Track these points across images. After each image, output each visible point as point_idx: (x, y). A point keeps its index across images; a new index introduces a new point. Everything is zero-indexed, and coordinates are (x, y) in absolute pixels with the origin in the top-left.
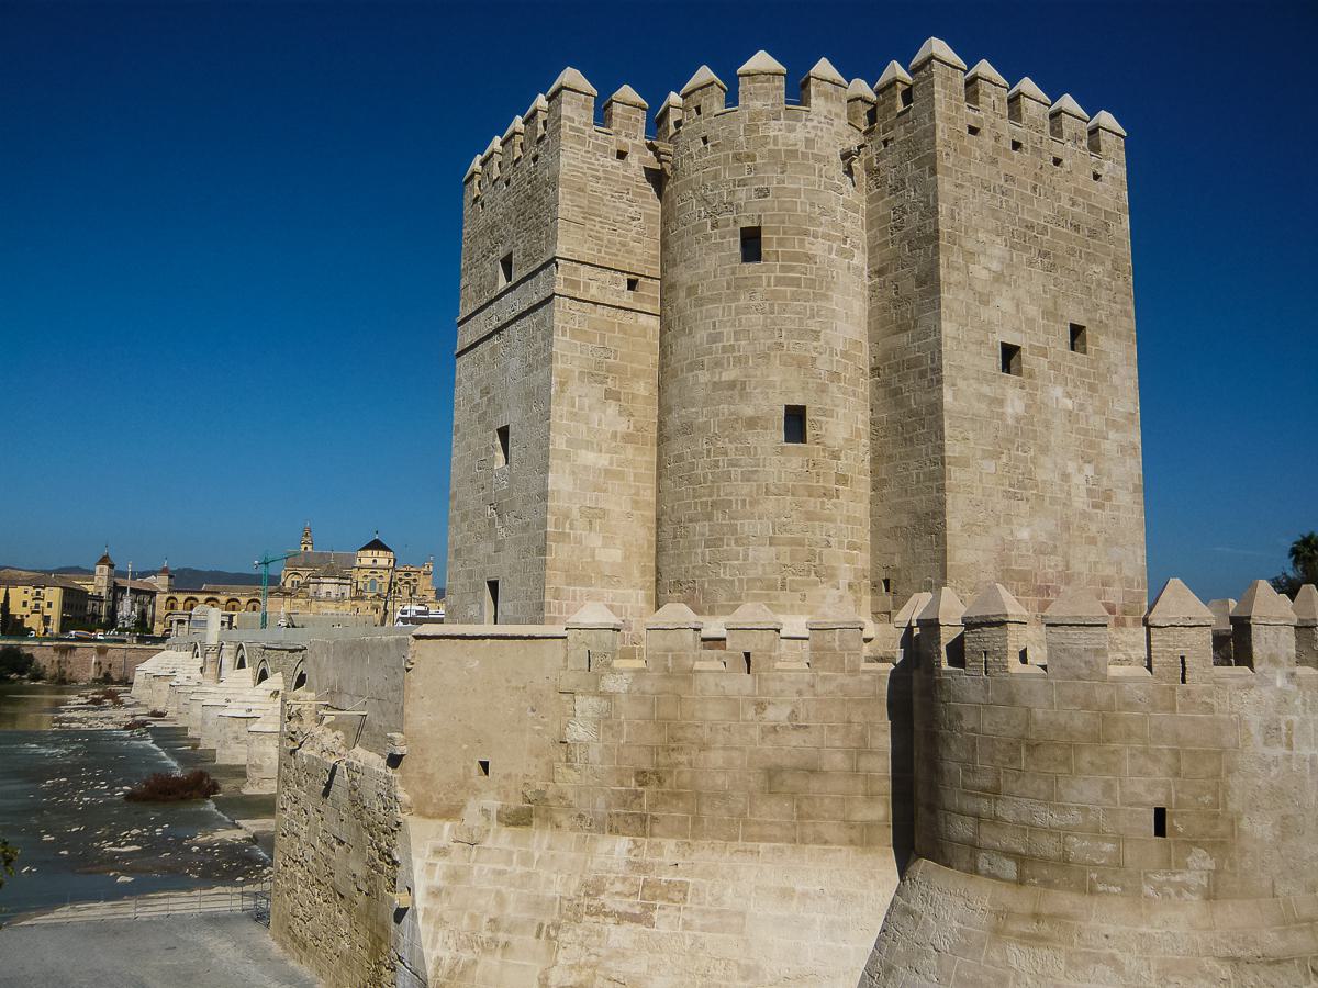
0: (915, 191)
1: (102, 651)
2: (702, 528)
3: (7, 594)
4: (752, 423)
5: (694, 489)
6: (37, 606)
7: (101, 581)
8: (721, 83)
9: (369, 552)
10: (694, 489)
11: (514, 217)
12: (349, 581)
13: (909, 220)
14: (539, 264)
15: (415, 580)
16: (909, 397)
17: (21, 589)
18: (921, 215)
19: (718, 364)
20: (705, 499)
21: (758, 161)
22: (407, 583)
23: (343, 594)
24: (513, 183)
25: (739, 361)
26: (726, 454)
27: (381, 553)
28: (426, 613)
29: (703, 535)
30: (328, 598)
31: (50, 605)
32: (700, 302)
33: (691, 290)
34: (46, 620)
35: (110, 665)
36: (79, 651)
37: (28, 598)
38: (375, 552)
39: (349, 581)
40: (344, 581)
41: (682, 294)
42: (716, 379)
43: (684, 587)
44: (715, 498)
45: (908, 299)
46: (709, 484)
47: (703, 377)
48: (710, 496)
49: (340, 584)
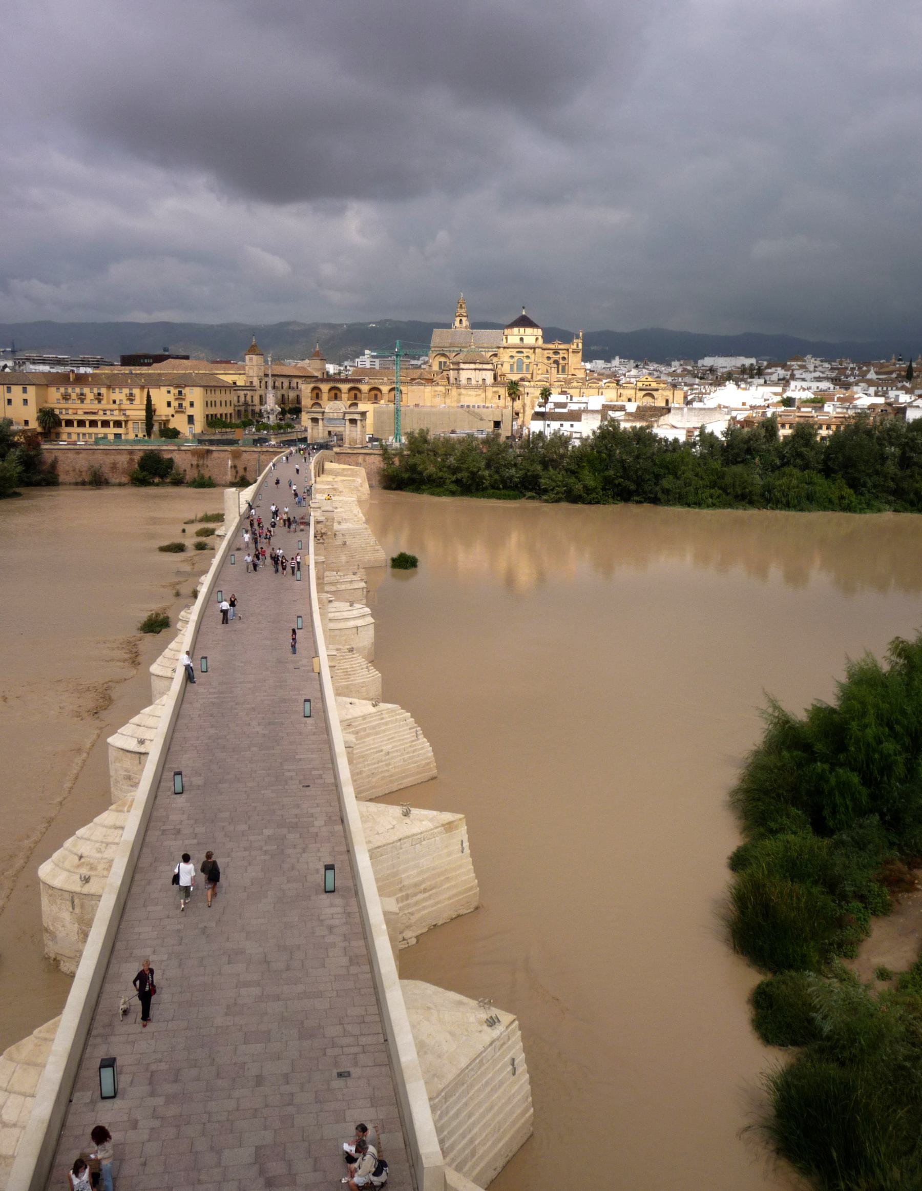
1: (236, 455)
3: (149, 397)
6: (180, 405)
7: (251, 371)
9: (516, 330)
12: (489, 366)
15: (564, 358)
17: (164, 389)
22: (556, 362)
23: (484, 380)
27: (529, 330)
28: (563, 405)
30: (469, 385)
31: (192, 404)
34: (191, 419)
35: (245, 469)
36: (215, 455)
37: (171, 397)
38: (522, 330)
39: (489, 366)
40: (485, 366)
49: (480, 370)
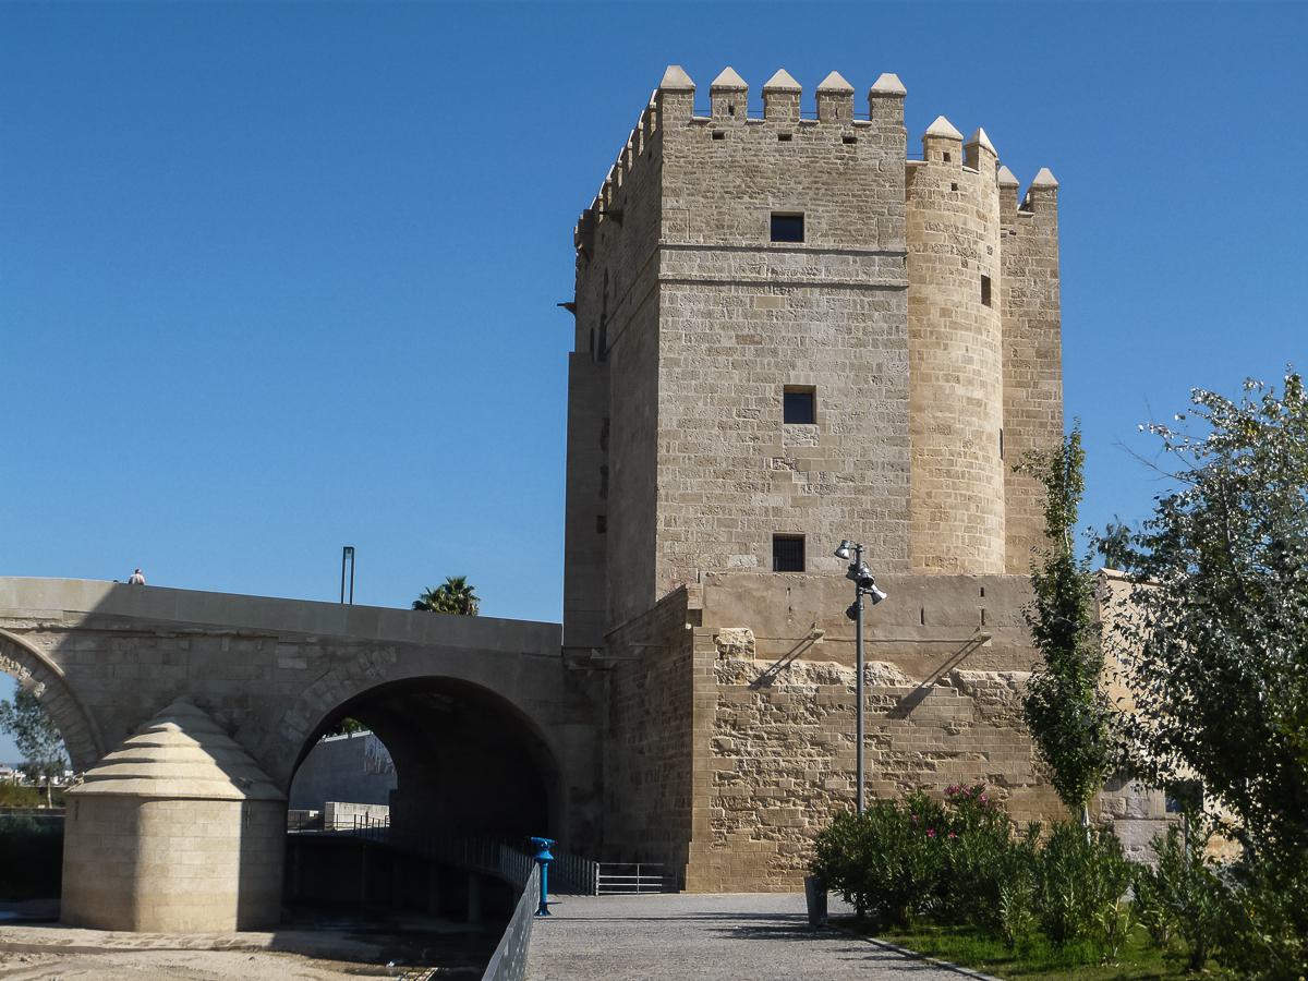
0: (1035, 282)
2: (962, 513)
4: (990, 437)
5: (953, 482)
8: (994, 151)
10: (953, 482)
11: (806, 182)
13: (1029, 304)
14: (874, 247)
16: (1029, 440)
18: (1042, 303)
19: (970, 382)
20: (963, 492)
21: (988, 224)
24: (798, 140)
25: (983, 384)
26: (977, 458)
29: (963, 521)
32: (955, 326)
33: (945, 313)
41: (934, 315)
42: (969, 395)
43: (946, 563)
44: (971, 493)
45: (1027, 364)
46: (966, 480)
47: (960, 390)
48: (968, 490)
